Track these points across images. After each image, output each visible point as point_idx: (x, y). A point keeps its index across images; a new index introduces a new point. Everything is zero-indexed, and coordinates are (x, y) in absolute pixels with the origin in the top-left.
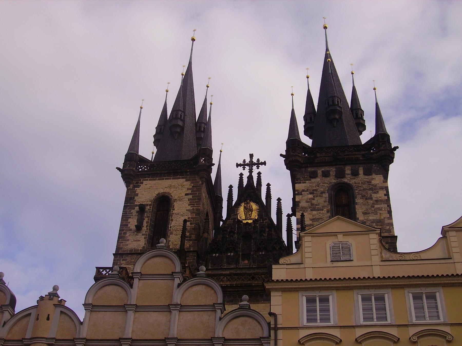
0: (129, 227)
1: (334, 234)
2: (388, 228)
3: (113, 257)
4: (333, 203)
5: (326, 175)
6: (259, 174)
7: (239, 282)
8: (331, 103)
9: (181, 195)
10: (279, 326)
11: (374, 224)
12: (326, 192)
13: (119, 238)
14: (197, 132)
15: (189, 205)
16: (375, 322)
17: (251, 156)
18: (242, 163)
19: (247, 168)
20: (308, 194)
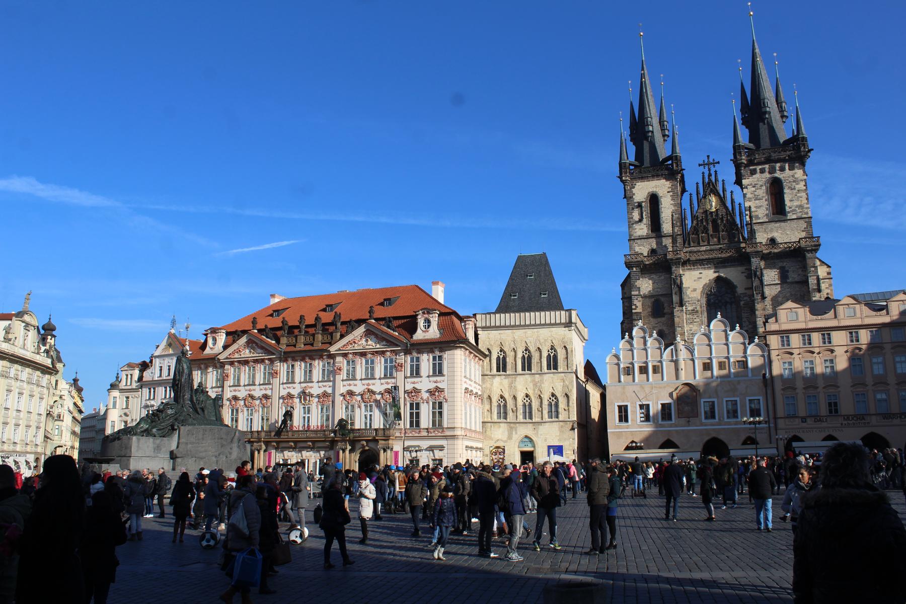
3: (627, 243)
5: (762, 171)
7: (714, 255)
13: (629, 227)
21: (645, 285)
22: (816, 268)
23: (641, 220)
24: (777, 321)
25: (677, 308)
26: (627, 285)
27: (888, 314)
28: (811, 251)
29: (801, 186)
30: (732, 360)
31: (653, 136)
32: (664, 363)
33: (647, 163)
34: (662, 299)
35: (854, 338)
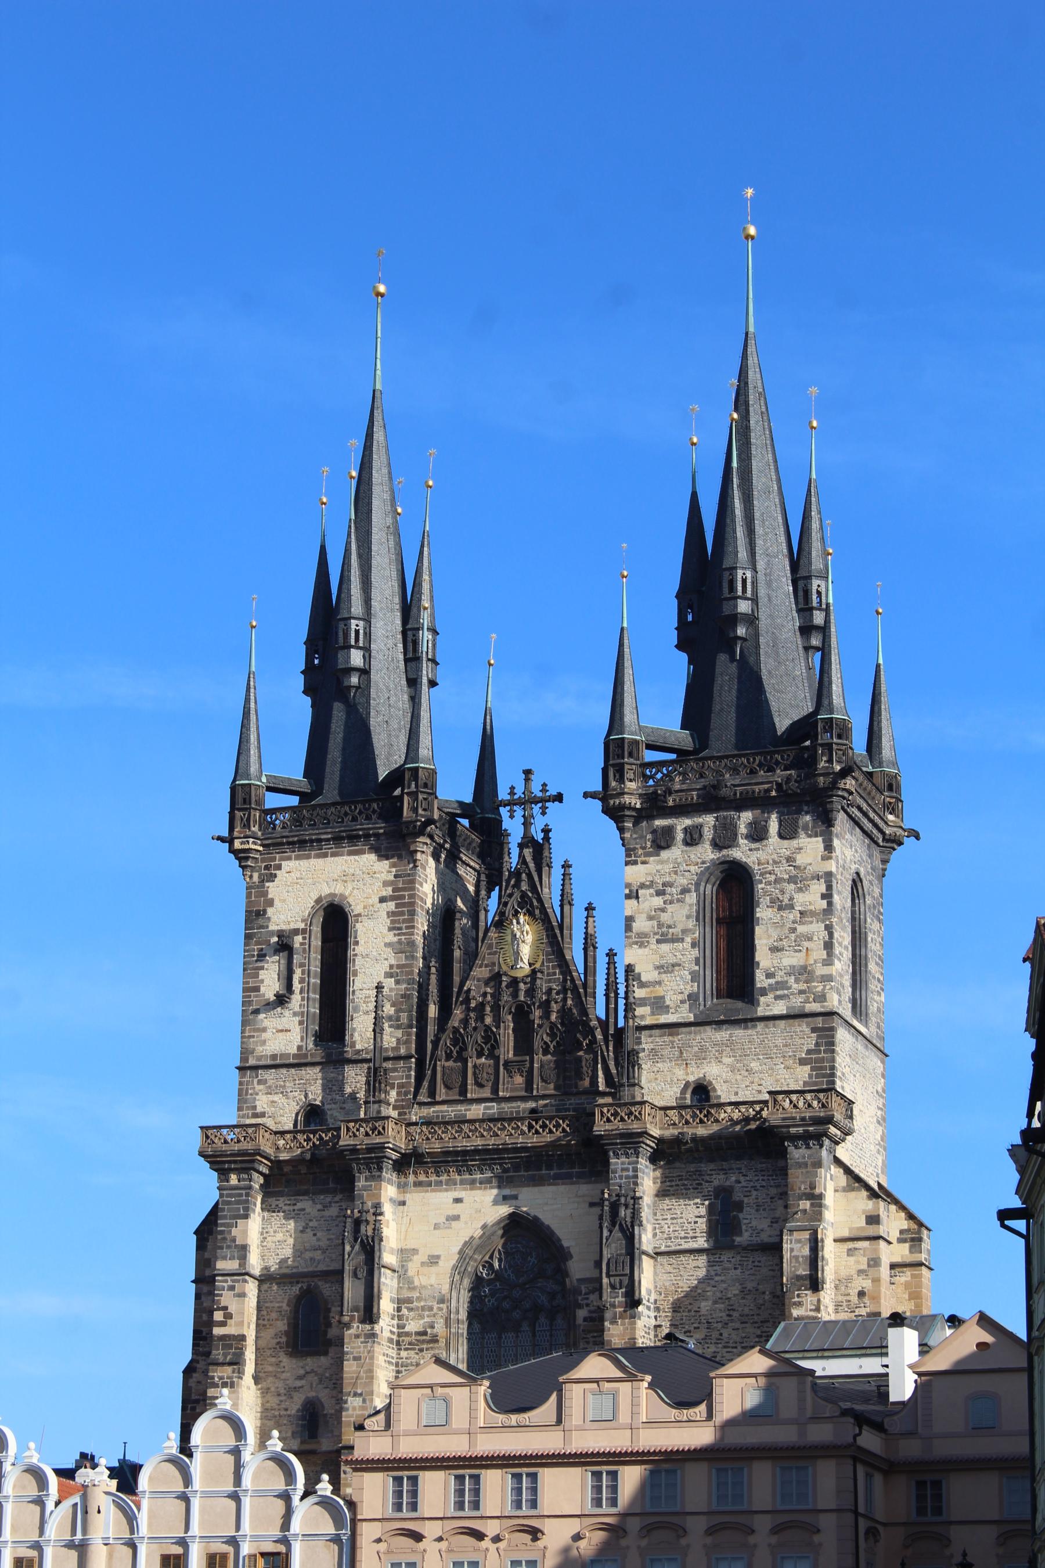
0: (264, 995)
1: (431, 1387)
2: (820, 989)
4: (708, 920)
6: (546, 831)
8: (726, 590)
9: (370, 901)
10: (359, 1517)
11: (792, 979)
12: (693, 888)
13: (245, 1023)
14: (406, 661)
15: (390, 929)
16: (467, 1512)
17: (528, 773)
18: (508, 797)
19: (519, 812)
20: (651, 895)
21: (266, 1238)
22: (817, 1200)
23: (281, 1000)
24: (388, 1425)
25: (356, 1328)
26: (210, 1233)
27: (710, 1416)
28: (806, 1137)
29: (812, 897)
30: (246, 1549)
31: (365, 688)
32: (49, 1552)
33: (331, 793)
34: (326, 1289)
35: (603, 1489)
